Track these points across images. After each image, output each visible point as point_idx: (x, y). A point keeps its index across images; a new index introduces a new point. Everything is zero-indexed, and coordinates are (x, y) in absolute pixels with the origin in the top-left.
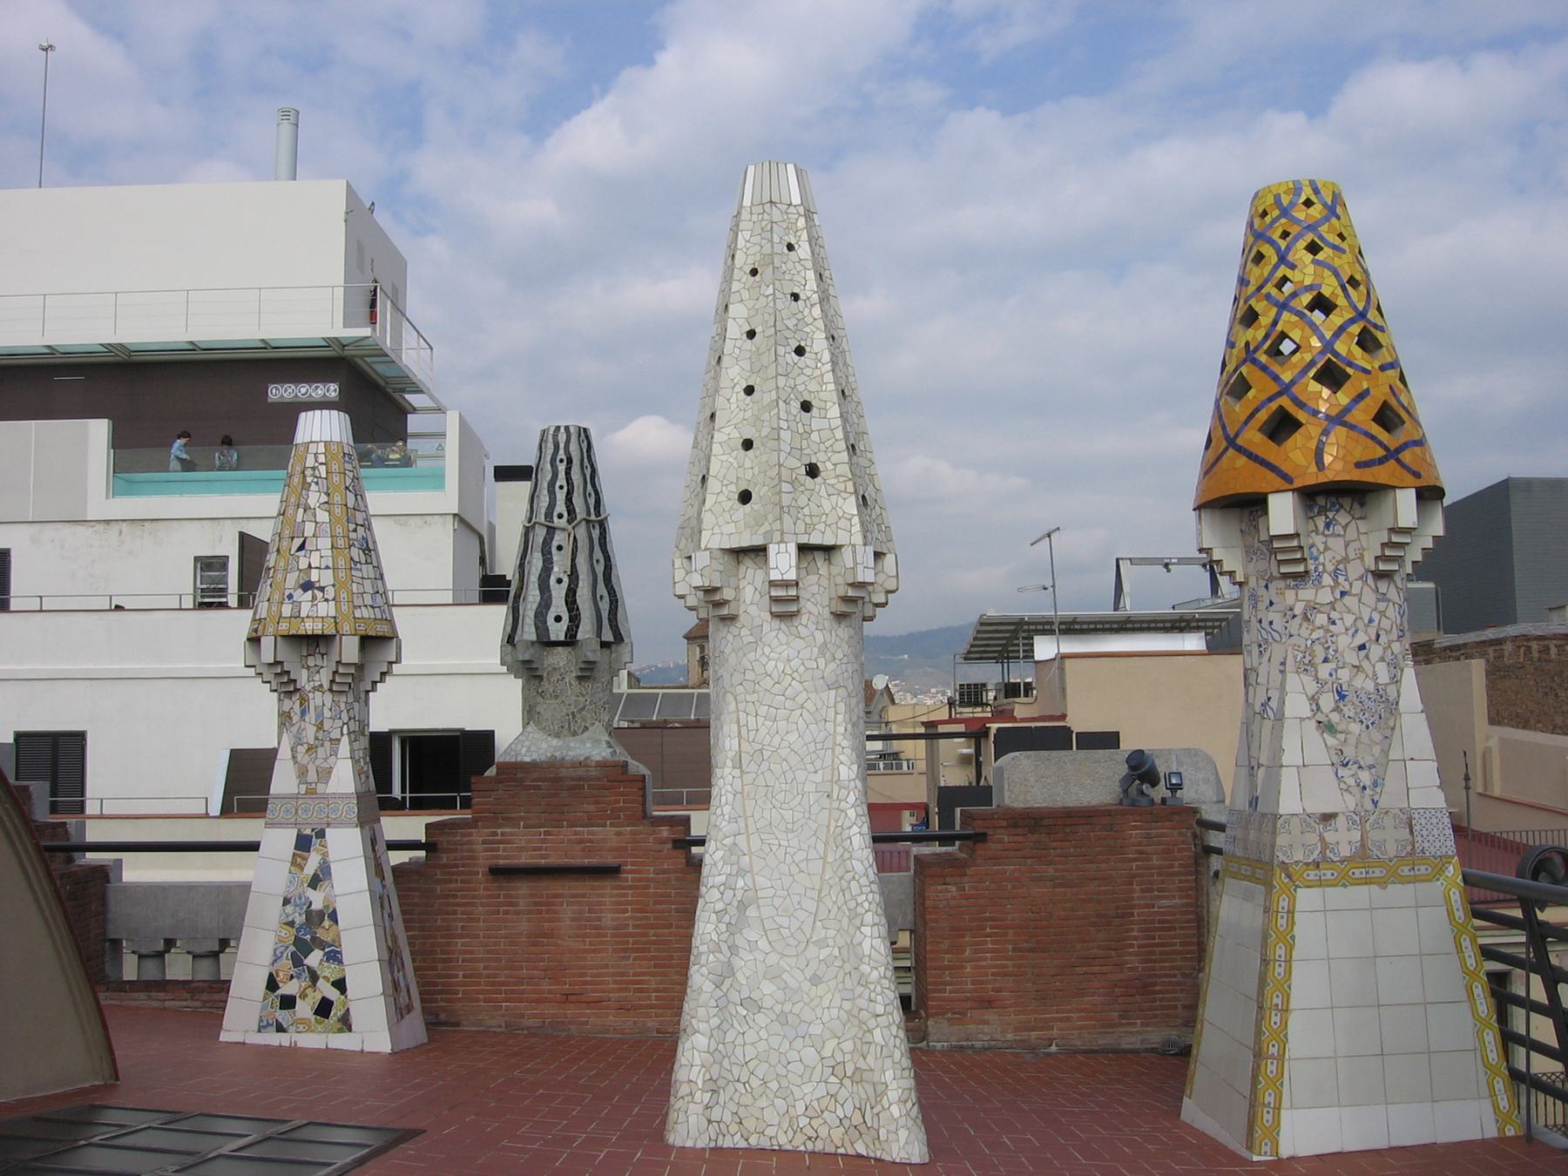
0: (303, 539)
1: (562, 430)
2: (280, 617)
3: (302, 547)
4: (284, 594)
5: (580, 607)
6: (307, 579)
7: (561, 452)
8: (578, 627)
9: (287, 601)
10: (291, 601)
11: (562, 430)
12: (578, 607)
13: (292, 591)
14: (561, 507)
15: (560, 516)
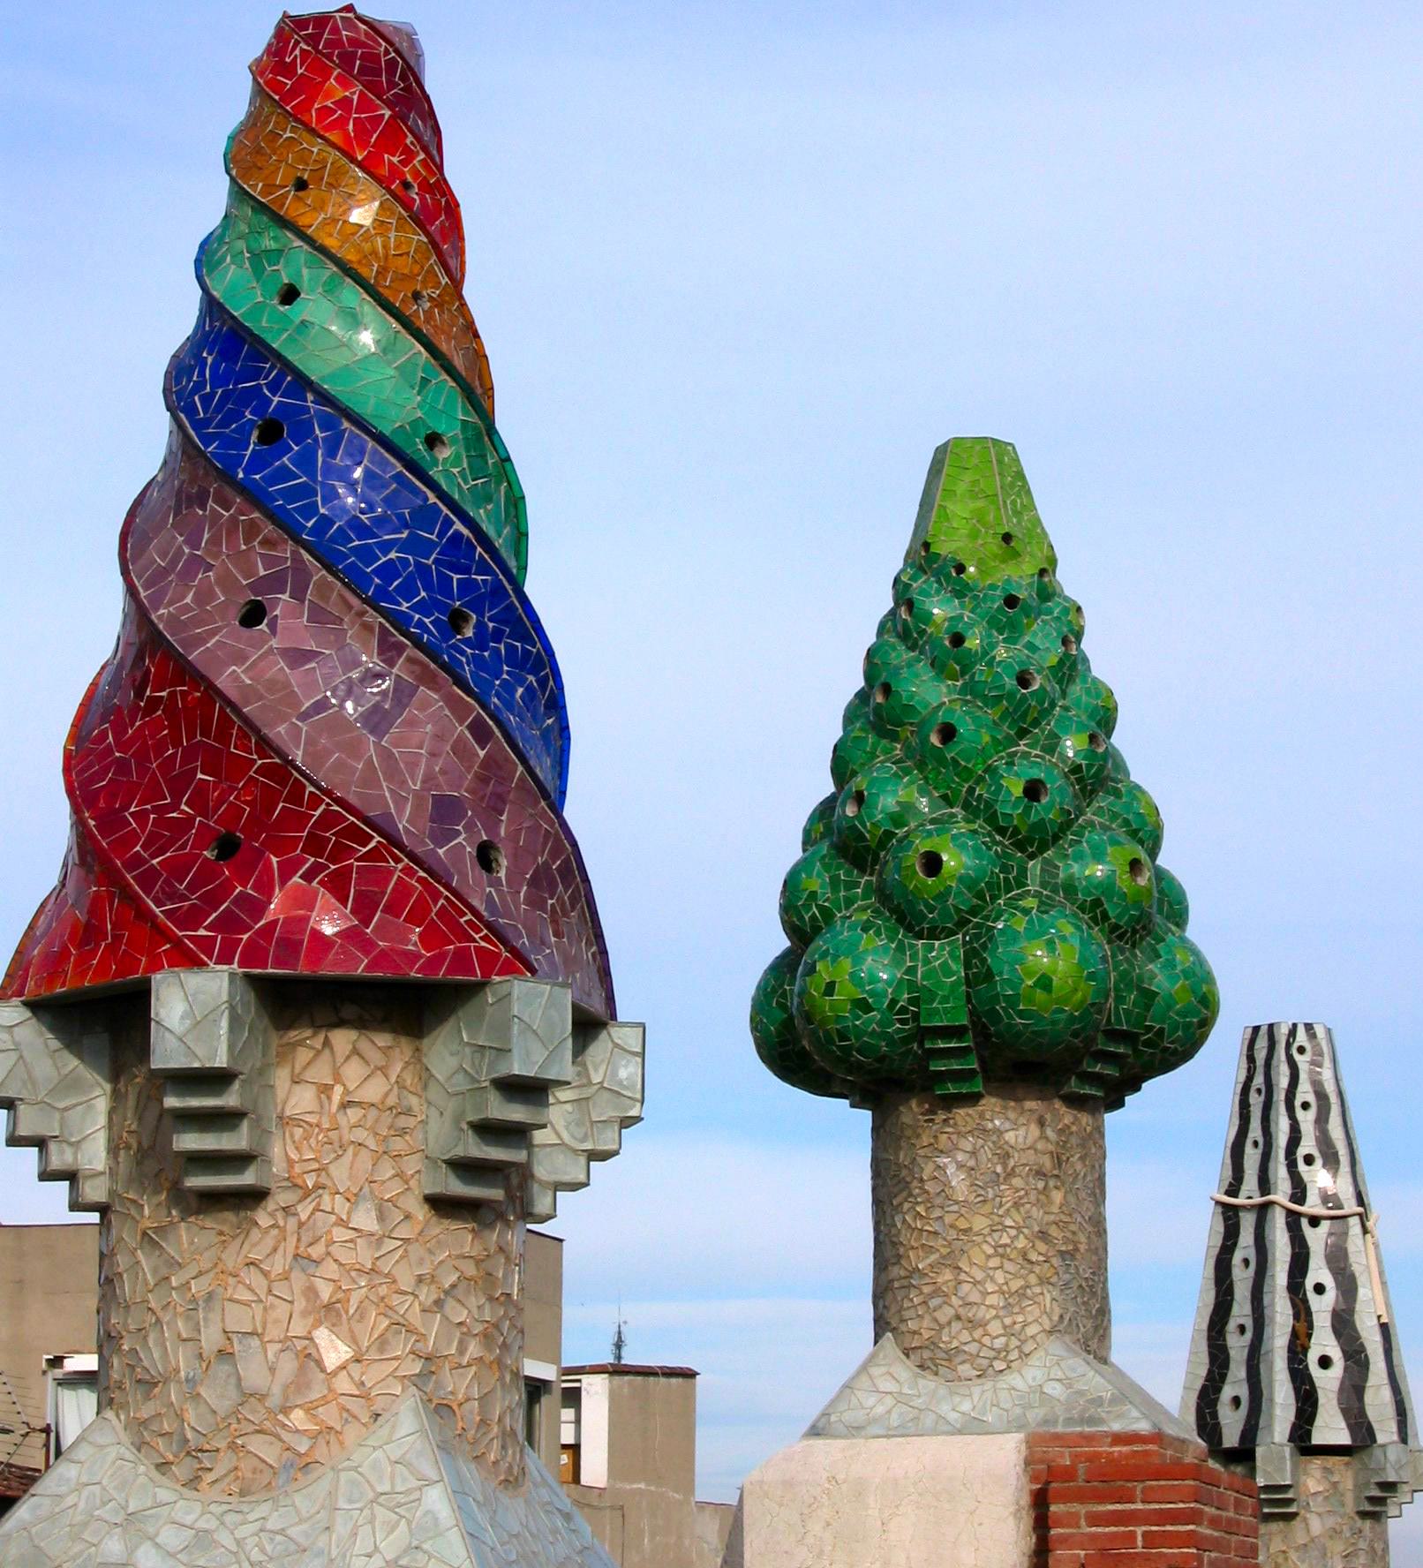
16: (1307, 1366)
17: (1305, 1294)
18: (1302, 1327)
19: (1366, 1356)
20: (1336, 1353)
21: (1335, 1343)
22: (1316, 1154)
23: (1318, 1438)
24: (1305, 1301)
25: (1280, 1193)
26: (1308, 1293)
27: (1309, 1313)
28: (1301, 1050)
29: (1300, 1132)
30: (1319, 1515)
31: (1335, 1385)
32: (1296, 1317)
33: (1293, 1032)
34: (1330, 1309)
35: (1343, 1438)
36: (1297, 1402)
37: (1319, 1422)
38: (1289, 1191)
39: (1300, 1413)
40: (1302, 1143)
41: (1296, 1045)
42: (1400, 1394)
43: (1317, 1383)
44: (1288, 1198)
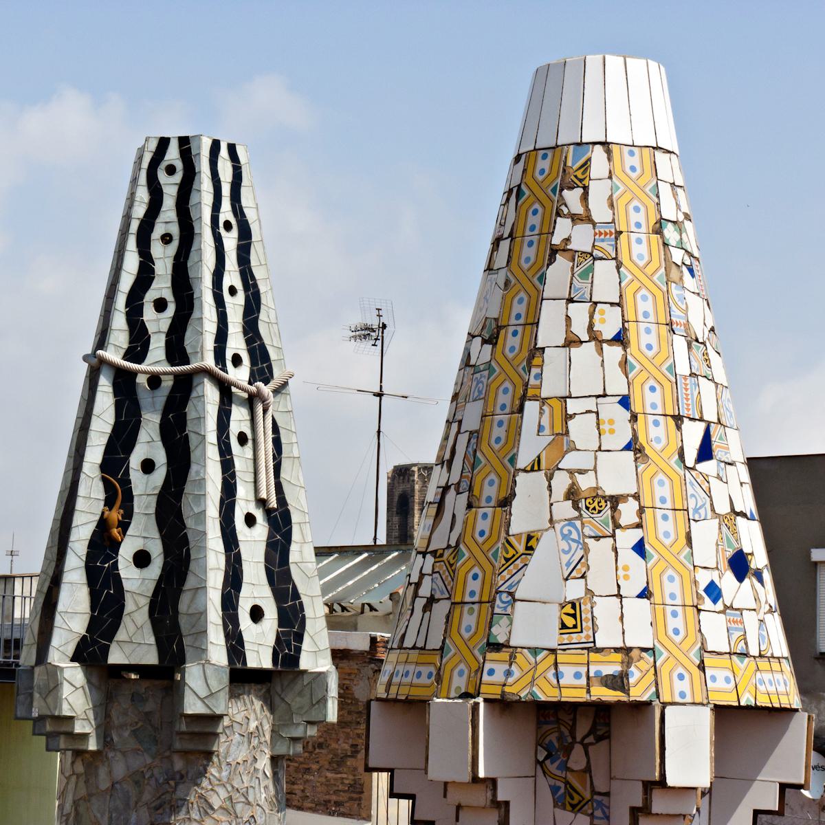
0: (702, 426)
1: (224, 152)
2: (703, 649)
3: (705, 452)
4: (696, 582)
5: (301, 589)
6: (736, 546)
7: (226, 205)
8: (299, 638)
9: (707, 604)
10: (719, 606)
11: (224, 152)
12: (295, 587)
13: (715, 575)
14: (236, 343)
15: (237, 360)
16: (115, 566)
17: (127, 472)
18: (115, 515)
19: (188, 551)
20: (156, 549)
21: (157, 535)
22: (168, 295)
23: (116, 657)
24: (126, 482)
25: (111, 348)
26: (132, 472)
27: (128, 497)
28: (171, 170)
29: (153, 271)
30: (124, 754)
31: (151, 587)
32: (109, 502)
33: (164, 143)
34: (157, 492)
35: (151, 657)
36: (93, 608)
37: (121, 635)
38: (126, 346)
39: (93, 625)
40: (154, 285)
41: (163, 165)
42: (296, 595)
43: (127, 585)
44: (122, 352)
